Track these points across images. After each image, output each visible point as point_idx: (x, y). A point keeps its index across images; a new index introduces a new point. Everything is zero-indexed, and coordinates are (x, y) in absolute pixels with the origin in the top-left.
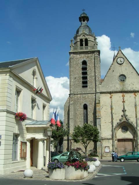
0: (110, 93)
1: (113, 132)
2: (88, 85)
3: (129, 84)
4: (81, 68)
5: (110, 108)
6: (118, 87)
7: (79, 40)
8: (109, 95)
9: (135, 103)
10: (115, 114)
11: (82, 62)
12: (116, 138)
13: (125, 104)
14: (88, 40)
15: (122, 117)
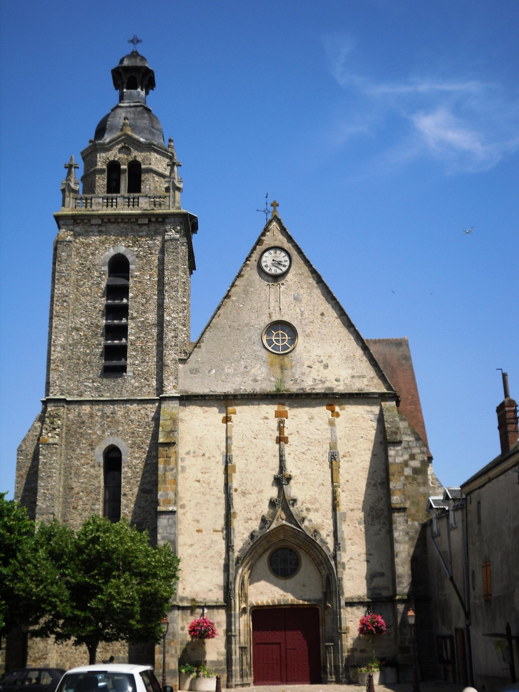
2: (129, 361)
3: (307, 364)
4: (103, 285)
5: (223, 467)
6: (260, 376)
7: (105, 167)
9: (333, 446)
10: (244, 494)
11: (108, 260)
12: (246, 601)
13: (287, 449)
14: (143, 167)
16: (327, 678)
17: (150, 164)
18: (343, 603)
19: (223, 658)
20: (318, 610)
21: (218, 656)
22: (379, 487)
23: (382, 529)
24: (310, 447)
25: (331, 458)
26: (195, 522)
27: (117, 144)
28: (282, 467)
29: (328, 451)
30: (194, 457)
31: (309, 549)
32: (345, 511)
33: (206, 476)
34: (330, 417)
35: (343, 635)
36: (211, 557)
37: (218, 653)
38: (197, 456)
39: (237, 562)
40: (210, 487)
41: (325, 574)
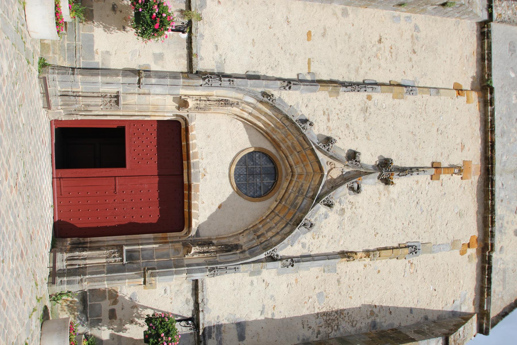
0: (484, 87)
1: (250, 82)
5: (399, 81)
8: (467, 73)
9: (430, 248)
10: (365, 110)
12: (198, 108)
13: (423, 178)
15: (344, 155)
16: (62, 251)
18: (197, 276)
19: (98, 61)
20: (181, 230)
21: (102, 52)
22: (370, 321)
23: (311, 330)
24: (425, 213)
25: (412, 246)
26: (323, 31)
28: (403, 171)
29: (420, 241)
30: (412, 36)
31: (281, 215)
32: (339, 271)
33: (387, 53)
34: (462, 243)
35: (142, 279)
36: (270, 53)
37: (107, 52)
38: (413, 43)
39: (264, 94)
40: (372, 58)
41: (241, 243)
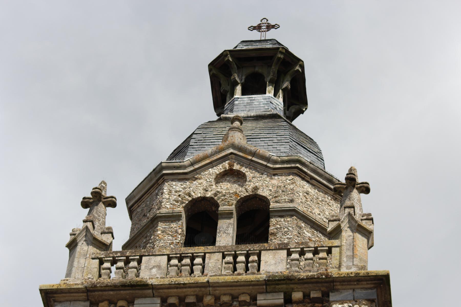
7: (180, 209)
14: (273, 205)
17: (292, 201)
27: (212, 164)
